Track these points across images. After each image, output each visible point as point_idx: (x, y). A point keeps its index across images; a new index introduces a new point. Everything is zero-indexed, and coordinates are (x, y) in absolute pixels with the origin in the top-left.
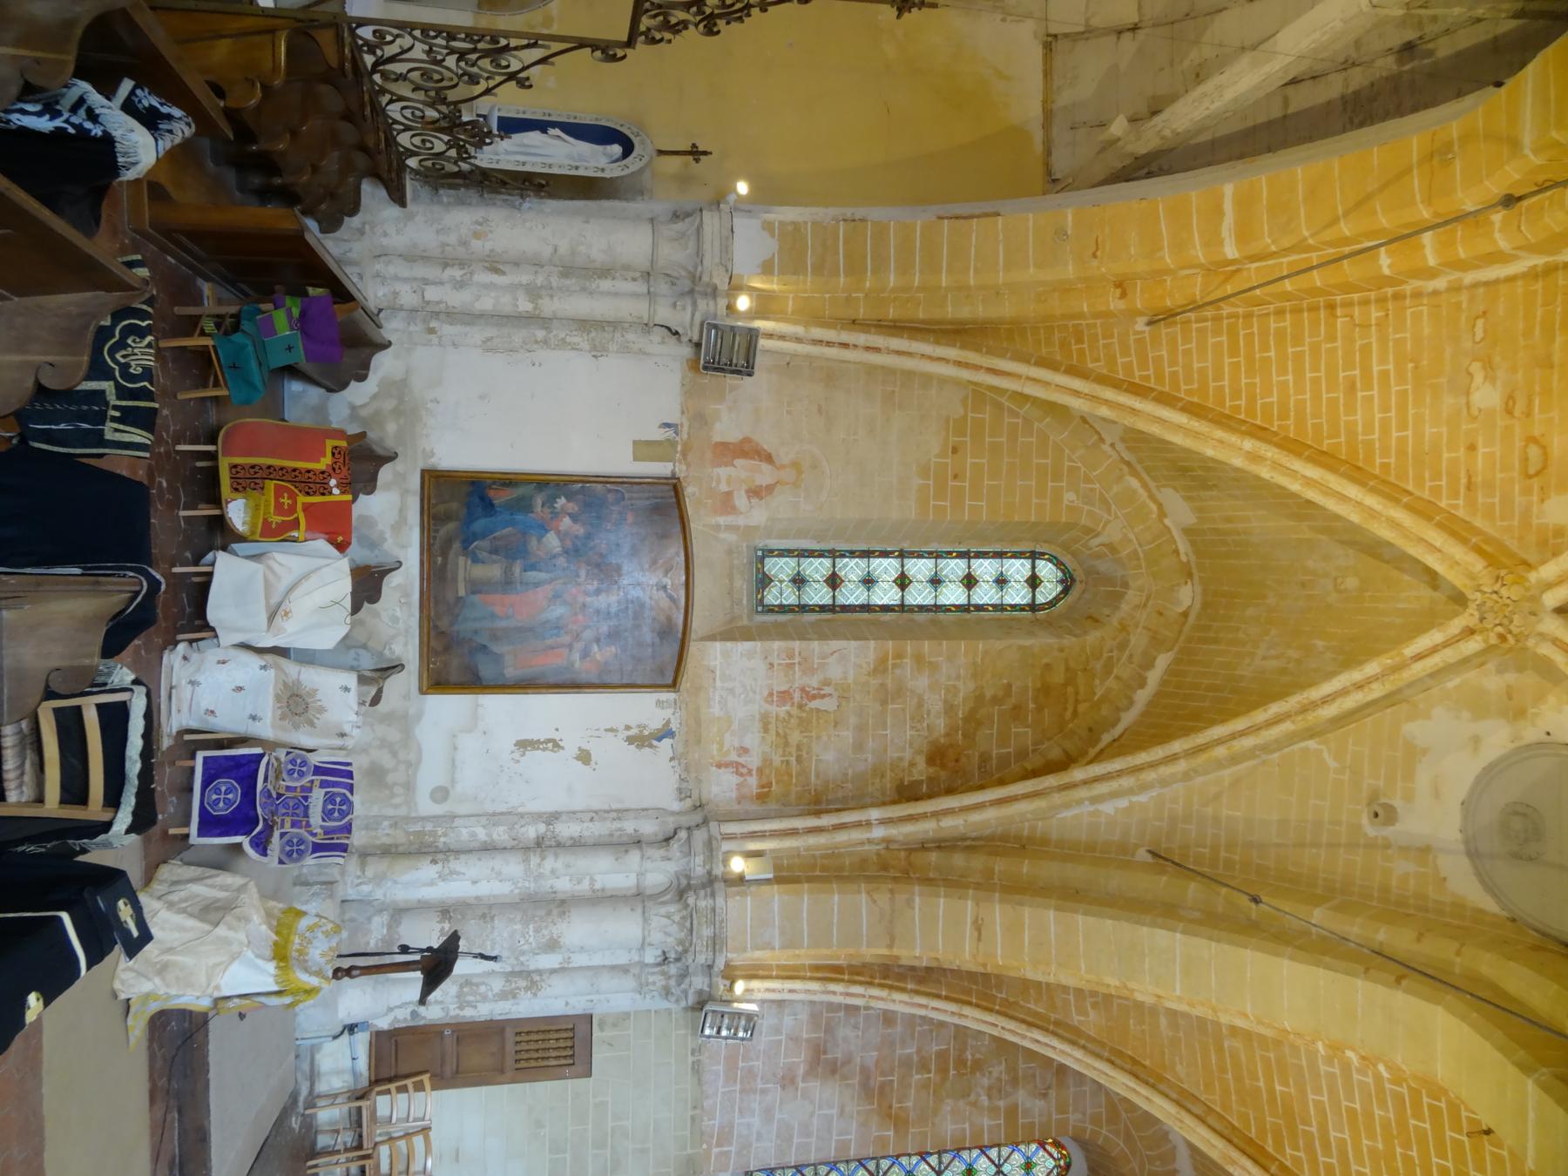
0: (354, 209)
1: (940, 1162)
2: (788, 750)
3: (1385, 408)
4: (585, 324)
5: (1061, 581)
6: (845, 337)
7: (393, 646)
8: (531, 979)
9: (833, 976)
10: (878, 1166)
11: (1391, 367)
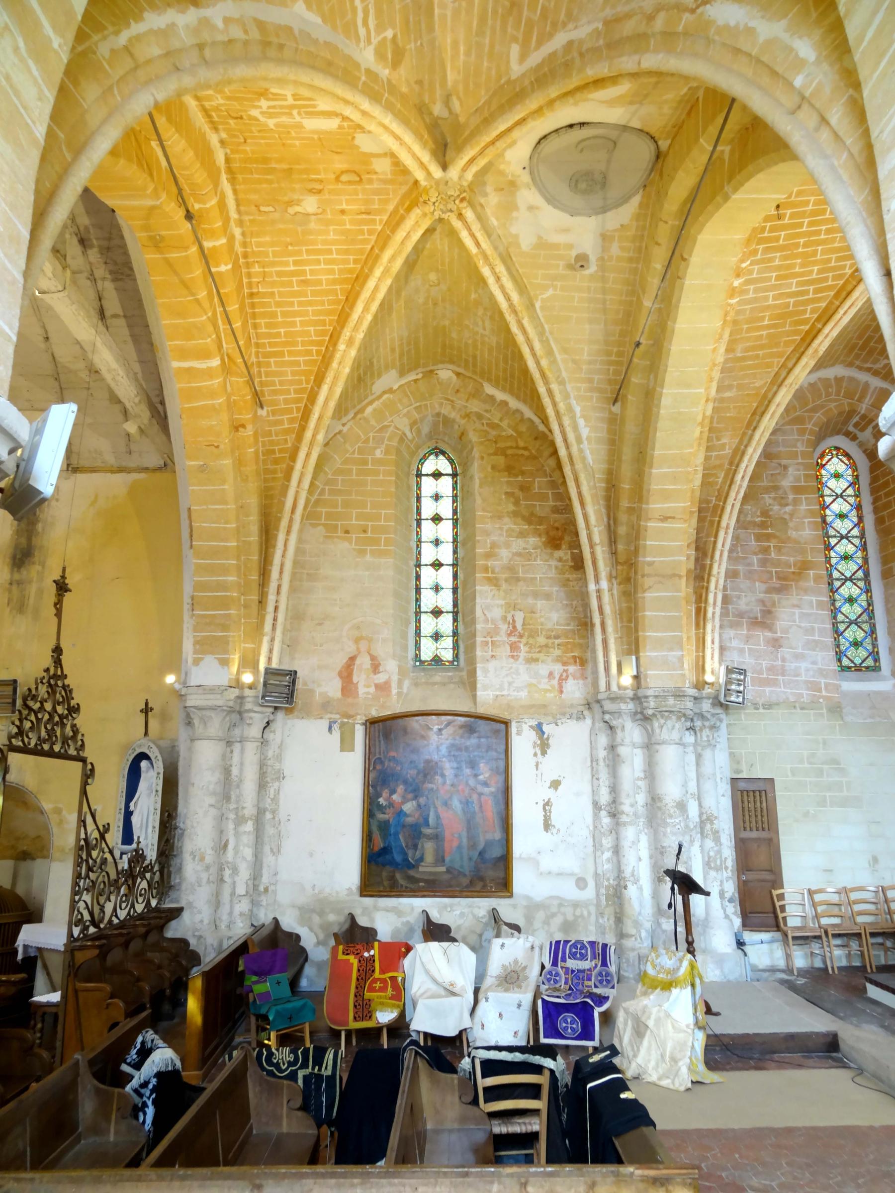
0: (184, 942)
1: (835, 536)
3: (318, 262)
4: (262, 785)
5: (437, 455)
6: (270, 608)
7: (480, 915)
8: (705, 820)
9: (702, 614)
10: (838, 579)
11: (291, 259)
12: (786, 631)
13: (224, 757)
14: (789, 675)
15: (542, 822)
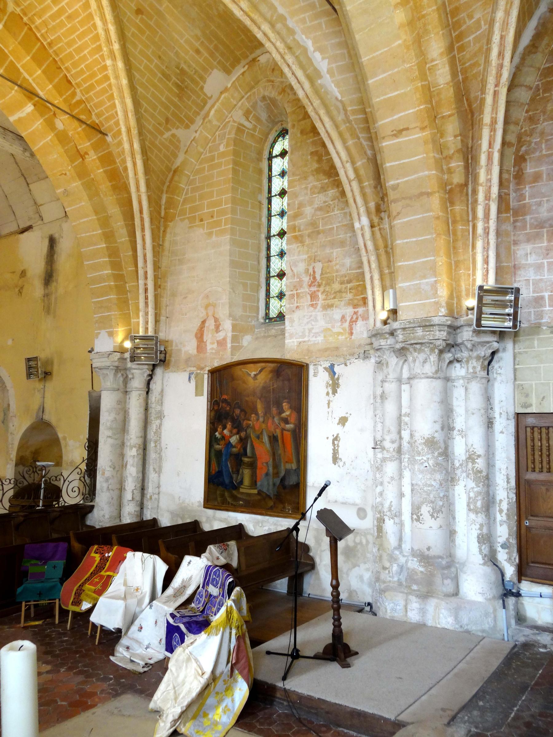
2: (343, 290)
13: (119, 402)
15: (331, 455)
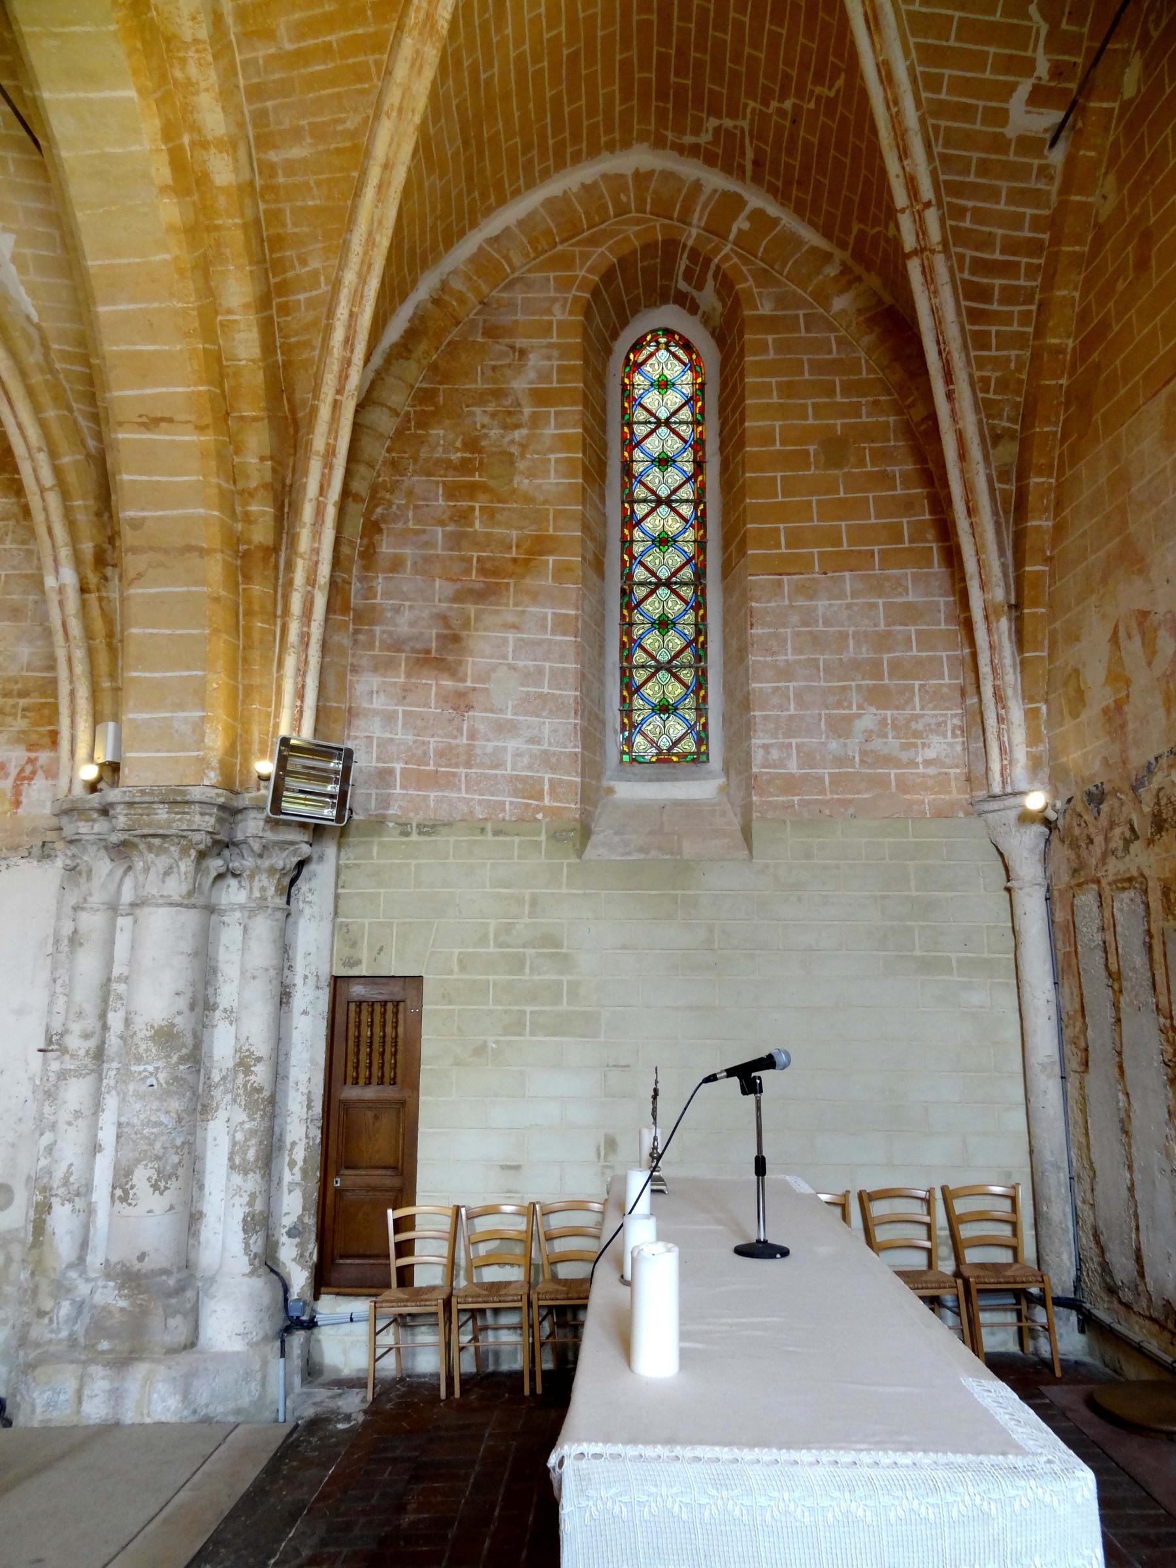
1: (645, 501)
2: (8, 709)
10: (642, 584)
12: (484, 677)
14: (482, 765)
